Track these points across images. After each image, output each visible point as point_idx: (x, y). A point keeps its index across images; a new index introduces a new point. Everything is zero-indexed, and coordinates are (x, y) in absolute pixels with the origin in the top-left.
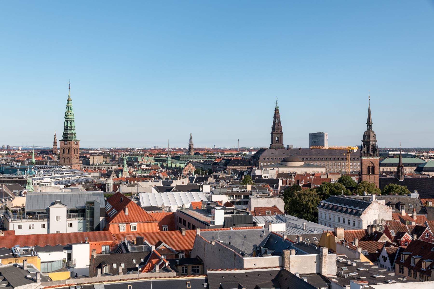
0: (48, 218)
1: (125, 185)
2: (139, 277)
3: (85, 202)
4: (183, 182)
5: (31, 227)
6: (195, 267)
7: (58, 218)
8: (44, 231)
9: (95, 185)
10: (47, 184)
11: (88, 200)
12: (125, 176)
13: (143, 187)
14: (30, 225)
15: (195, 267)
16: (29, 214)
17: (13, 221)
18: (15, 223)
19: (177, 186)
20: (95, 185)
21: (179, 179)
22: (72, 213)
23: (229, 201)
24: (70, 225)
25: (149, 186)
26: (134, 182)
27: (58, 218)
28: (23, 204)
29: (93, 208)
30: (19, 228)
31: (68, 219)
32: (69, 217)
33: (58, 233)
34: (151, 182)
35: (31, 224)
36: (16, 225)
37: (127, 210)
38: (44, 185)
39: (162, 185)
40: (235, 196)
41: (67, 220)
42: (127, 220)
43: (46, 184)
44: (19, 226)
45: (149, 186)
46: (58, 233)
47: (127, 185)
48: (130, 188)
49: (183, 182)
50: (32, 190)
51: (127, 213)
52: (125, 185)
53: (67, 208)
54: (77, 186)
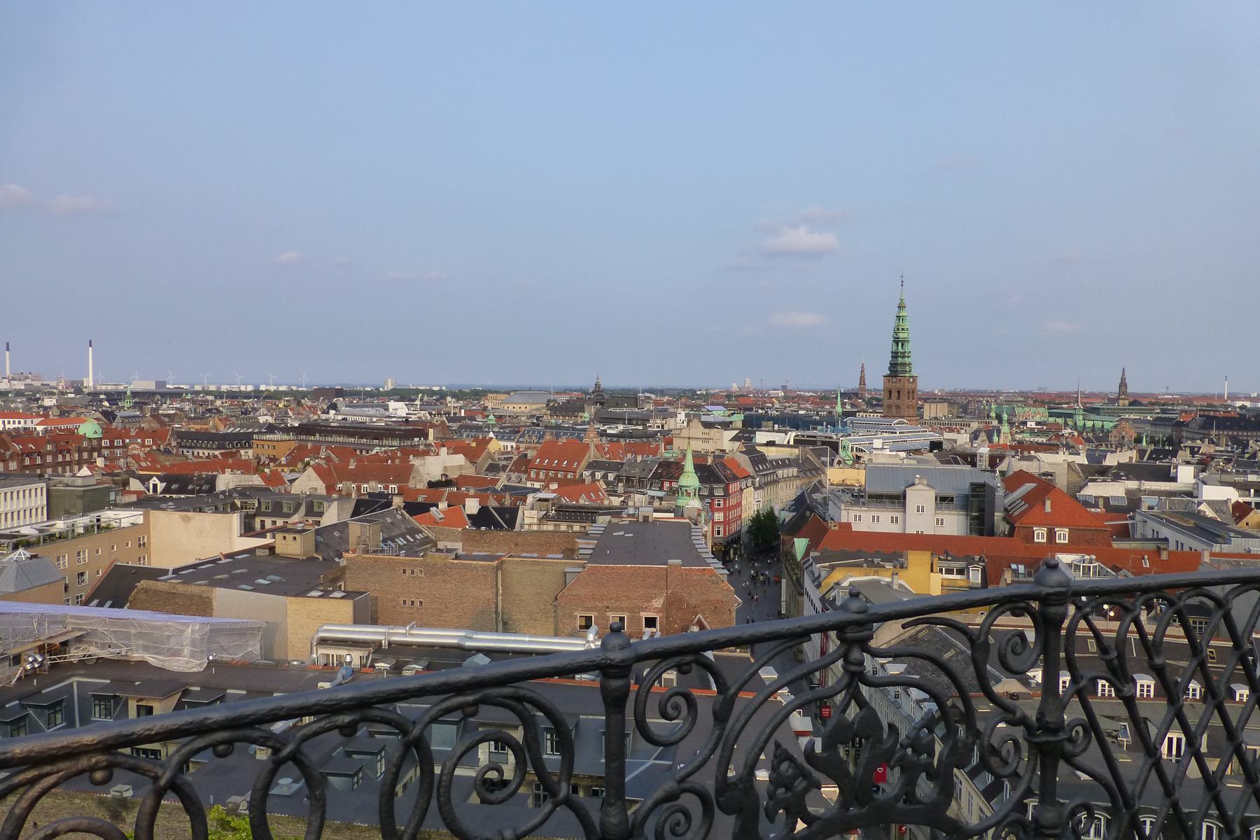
0: (904, 505)
1: (1013, 457)
2: (1109, 628)
4: (1131, 458)
6: (1201, 623)
7: (920, 509)
8: (895, 529)
13: (1049, 464)
15: (1201, 623)
16: (871, 496)
19: (1121, 466)
21: (1118, 451)
22: (943, 500)
23: (1241, 500)
24: (940, 522)
25: (1062, 462)
26: (1029, 453)
28: (843, 481)
31: (937, 512)
36: (852, 514)
37: (1048, 503)
40: (1252, 491)
41: (935, 514)
45: (1062, 462)
47: (1017, 457)
49: (1131, 458)
51: (1048, 509)
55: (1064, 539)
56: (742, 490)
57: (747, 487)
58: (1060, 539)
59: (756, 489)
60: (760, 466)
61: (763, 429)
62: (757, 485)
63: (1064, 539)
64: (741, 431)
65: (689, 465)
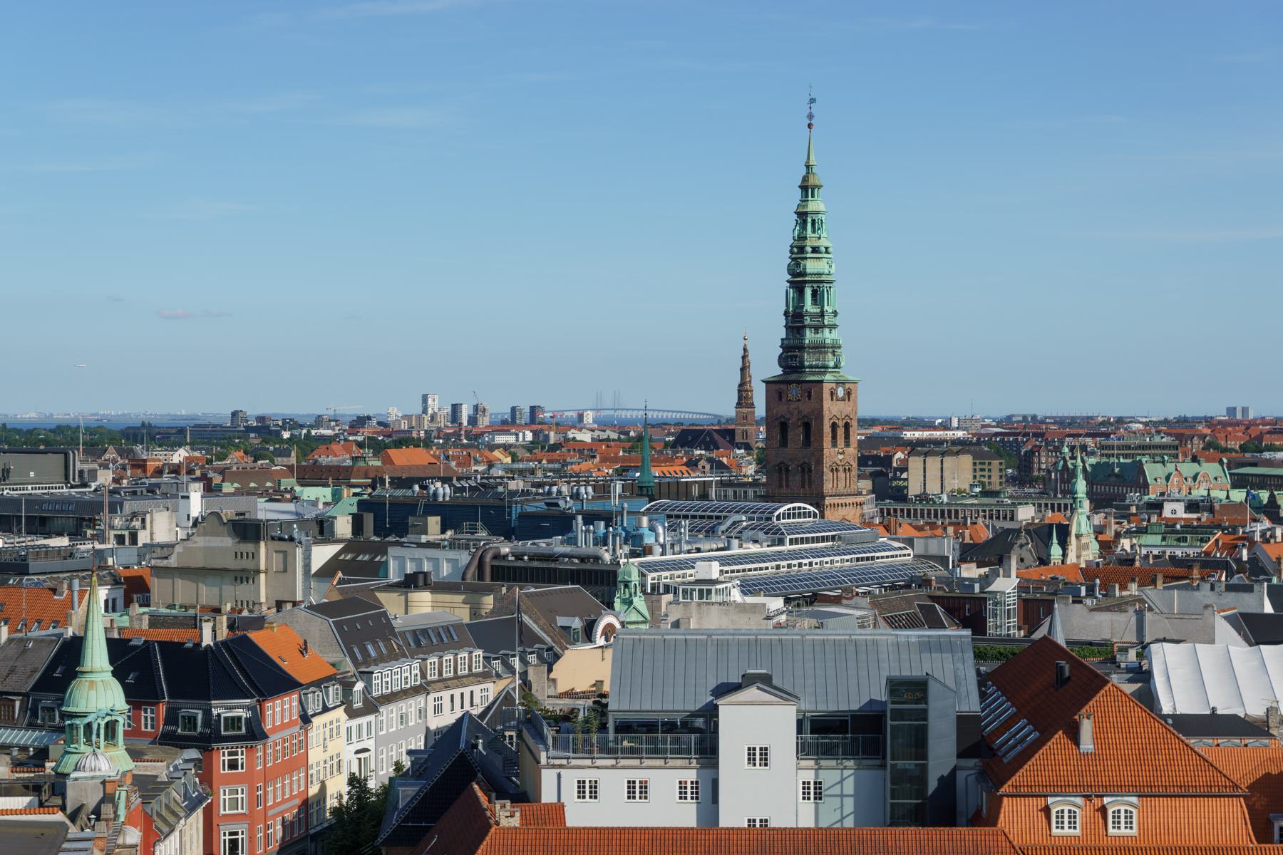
0: (708, 752)
3: (884, 682)
5: (638, 791)
7: (759, 756)
9: (933, 598)
10: (709, 592)
11: (895, 673)
12: (1078, 557)
14: (631, 784)
16: (625, 728)
17: (557, 762)
18: (563, 772)
20: (933, 598)
27: (759, 756)
29: (924, 715)
30: (581, 794)
31: (803, 763)
32: (804, 750)
33: (758, 826)
34: (1212, 589)
35: (638, 775)
36: (571, 778)
37: (1087, 728)
38: (696, 594)
39: (1268, 608)
42: (1088, 780)
43: (701, 591)
44: (581, 784)
46: (758, 826)
47: (1089, 602)
48: (1105, 617)
50: (641, 619)
51: (1087, 744)
52: (1081, 602)
53: (798, 711)
54: (844, 602)
55: (1129, 825)
56: (306, 719)
57: (326, 709)
58: (1117, 824)
59: (352, 714)
60: (370, 647)
61: (411, 537)
62: (358, 704)
63: (1129, 825)
64: (350, 546)
65: (97, 657)
